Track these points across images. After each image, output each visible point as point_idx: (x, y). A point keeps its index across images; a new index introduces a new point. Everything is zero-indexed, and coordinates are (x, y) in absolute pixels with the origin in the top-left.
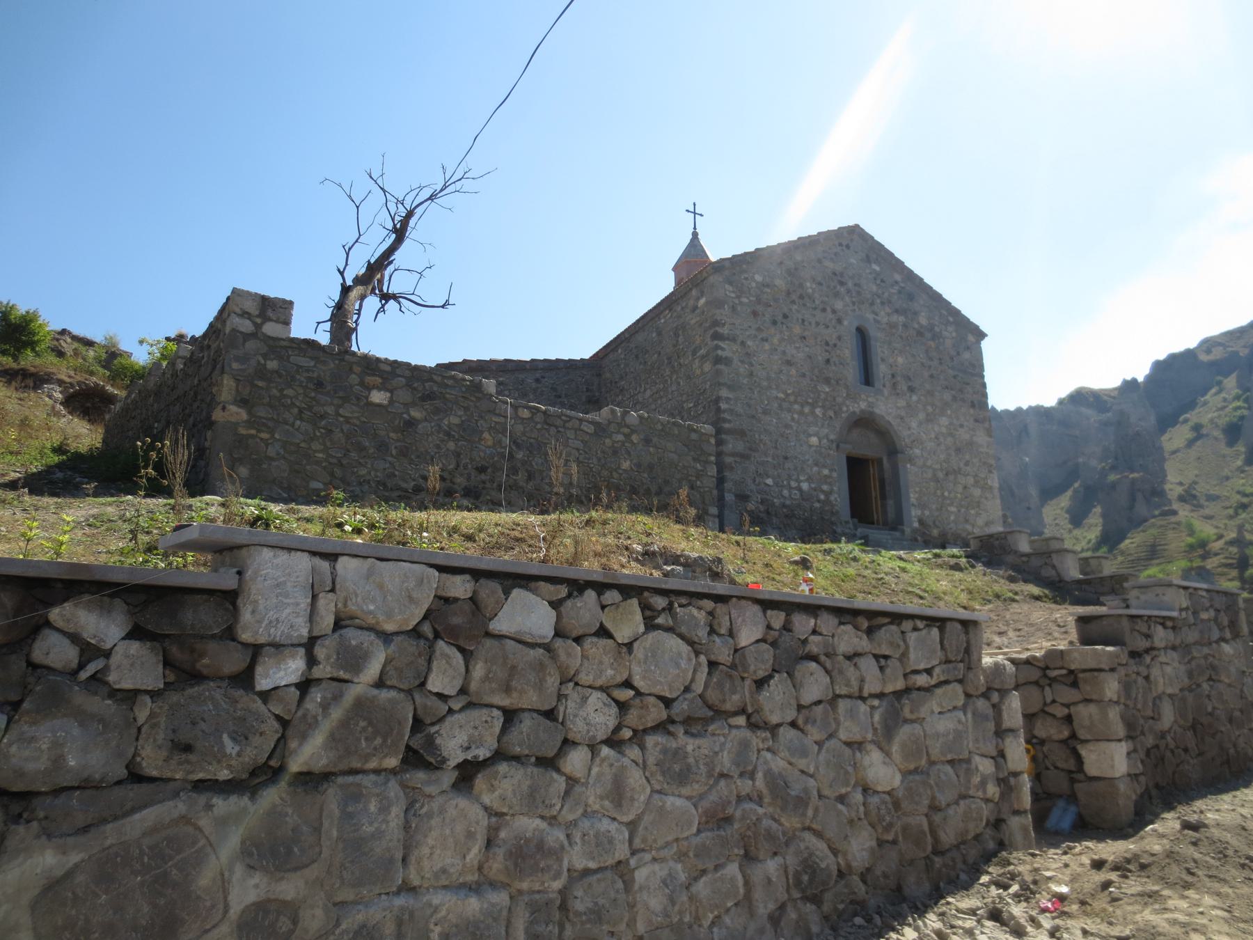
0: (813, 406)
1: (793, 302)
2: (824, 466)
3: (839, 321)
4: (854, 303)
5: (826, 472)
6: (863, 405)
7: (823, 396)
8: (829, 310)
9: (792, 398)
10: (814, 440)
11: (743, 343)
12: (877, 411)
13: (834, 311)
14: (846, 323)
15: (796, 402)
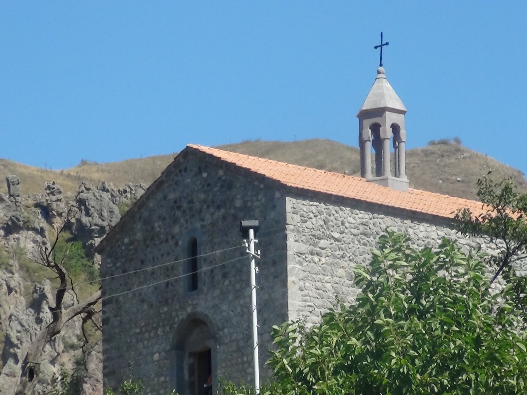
0: (156, 329)
1: (147, 246)
2: (162, 375)
3: (177, 244)
4: (187, 221)
5: (162, 379)
6: (189, 310)
7: (163, 316)
8: (170, 237)
9: (144, 330)
10: (156, 357)
11: (117, 301)
12: (199, 309)
13: (173, 237)
14: (180, 243)
15: (146, 331)
